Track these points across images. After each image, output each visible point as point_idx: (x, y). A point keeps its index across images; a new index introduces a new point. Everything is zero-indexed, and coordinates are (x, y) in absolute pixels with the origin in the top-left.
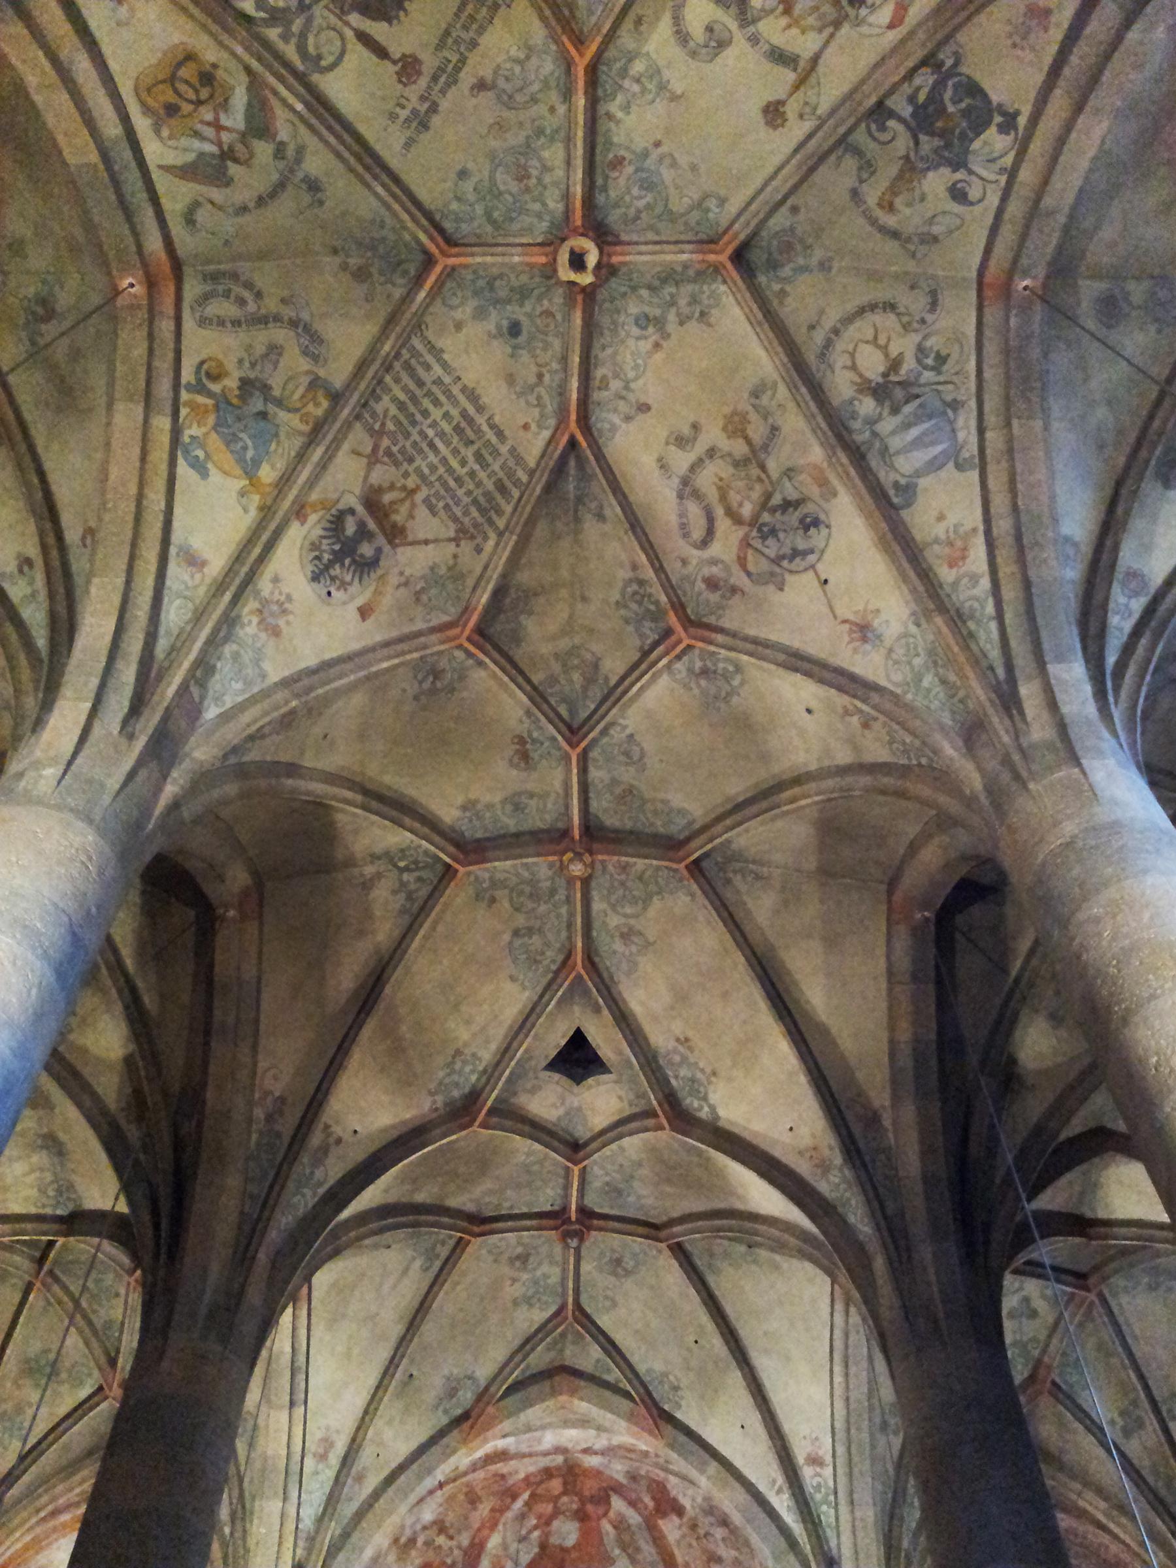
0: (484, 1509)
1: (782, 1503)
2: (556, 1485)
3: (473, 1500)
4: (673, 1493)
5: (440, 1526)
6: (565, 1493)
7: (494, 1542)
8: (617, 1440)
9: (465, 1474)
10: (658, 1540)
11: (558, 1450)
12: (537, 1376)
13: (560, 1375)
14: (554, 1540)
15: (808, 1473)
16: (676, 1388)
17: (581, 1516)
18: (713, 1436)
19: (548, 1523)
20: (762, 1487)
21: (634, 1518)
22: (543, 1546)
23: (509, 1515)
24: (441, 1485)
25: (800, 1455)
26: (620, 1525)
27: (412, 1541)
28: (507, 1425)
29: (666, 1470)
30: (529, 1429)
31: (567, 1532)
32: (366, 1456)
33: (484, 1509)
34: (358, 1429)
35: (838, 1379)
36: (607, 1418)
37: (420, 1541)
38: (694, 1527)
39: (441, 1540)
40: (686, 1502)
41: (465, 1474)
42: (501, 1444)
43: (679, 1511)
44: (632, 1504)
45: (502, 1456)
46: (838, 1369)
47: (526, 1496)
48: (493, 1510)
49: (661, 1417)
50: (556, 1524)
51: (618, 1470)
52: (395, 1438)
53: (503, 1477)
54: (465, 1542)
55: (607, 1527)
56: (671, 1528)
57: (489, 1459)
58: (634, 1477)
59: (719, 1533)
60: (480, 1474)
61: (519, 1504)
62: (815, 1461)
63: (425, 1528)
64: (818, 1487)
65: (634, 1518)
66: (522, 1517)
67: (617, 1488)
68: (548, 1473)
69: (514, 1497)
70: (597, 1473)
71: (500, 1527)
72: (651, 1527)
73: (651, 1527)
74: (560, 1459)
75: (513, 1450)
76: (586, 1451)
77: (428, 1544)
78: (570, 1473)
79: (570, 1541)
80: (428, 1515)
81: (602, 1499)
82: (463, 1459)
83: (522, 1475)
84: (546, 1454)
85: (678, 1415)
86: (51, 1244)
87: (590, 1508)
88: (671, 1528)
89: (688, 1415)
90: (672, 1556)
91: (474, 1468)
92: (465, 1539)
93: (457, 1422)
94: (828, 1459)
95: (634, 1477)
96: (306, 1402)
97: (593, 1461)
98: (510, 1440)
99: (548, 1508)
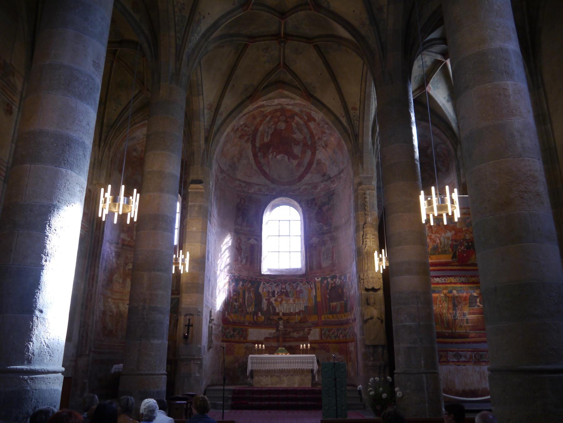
0: (258, 120)
1: (344, 120)
2: (279, 114)
3: (254, 118)
4: (313, 116)
5: (246, 125)
6: (281, 115)
7: (261, 128)
8: (296, 102)
9: (252, 111)
10: (308, 128)
11: (279, 104)
12: (272, 82)
13: (280, 84)
14: (278, 128)
15: (352, 112)
16: (314, 88)
17: (286, 122)
18: (325, 101)
19: (277, 123)
20: (338, 115)
21: (301, 122)
22: (275, 129)
23: (265, 122)
24: (245, 115)
25: (350, 106)
26: (297, 124)
27: (238, 129)
28: (264, 98)
29: (311, 110)
30: (270, 99)
31: (282, 126)
32: (222, 109)
33: (258, 120)
34: (219, 101)
35: (363, 86)
36: (294, 96)
37: (240, 129)
38: (319, 124)
39: (246, 128)
40: (317, 118)
41: (252, 111)
42: (262, 103)
43: (315, 120)
44: (301, 118)
45: (263, 106)
46: (363, 83)
47: (270, 116)
48: (260, 120)
49: (309, 95)
50: (279, 123)
51: (297, 110)
52: (229, 102)
53: (263, 112)
54: (253, 129)
55: (293, 124)
56: (312, 125)
57: (258, 107)
58: (302, 111)
59: (326, 126)
60: (256, 111)
61: (268, 119)
62: (354, 109)
63: (241, 126)
64: (354, 116)
65: (301, 122)
66: (269, 122)
67: (297, 114)
68: (276, 111)
69: (266, 117)
70: (290, 110)
71: (263, 125)
72: (306, 124)
73: (306, 124)
74: (279, 107)
75: (265, 104)
76: (287, 105)
77: (242, 130)
78: (283, 111)
79: (283, 128)
80: (242, 123)
81: (292, 117)
82: (250, 108)
83: (268, 111)
84: (275, 105)
85: (315, 95)
86: (117, 50)
87: (288, 120)
88: (312, 125)
89: (318, 95)
90: (312, 132)
91: (254, 109)
92: (253, 128)
93: (248, 98)
94: (358, 108)
95: (302, 111)
96: (203, 94)
97: (290, 107)
98: (265, 102)
99: (276, 120)
